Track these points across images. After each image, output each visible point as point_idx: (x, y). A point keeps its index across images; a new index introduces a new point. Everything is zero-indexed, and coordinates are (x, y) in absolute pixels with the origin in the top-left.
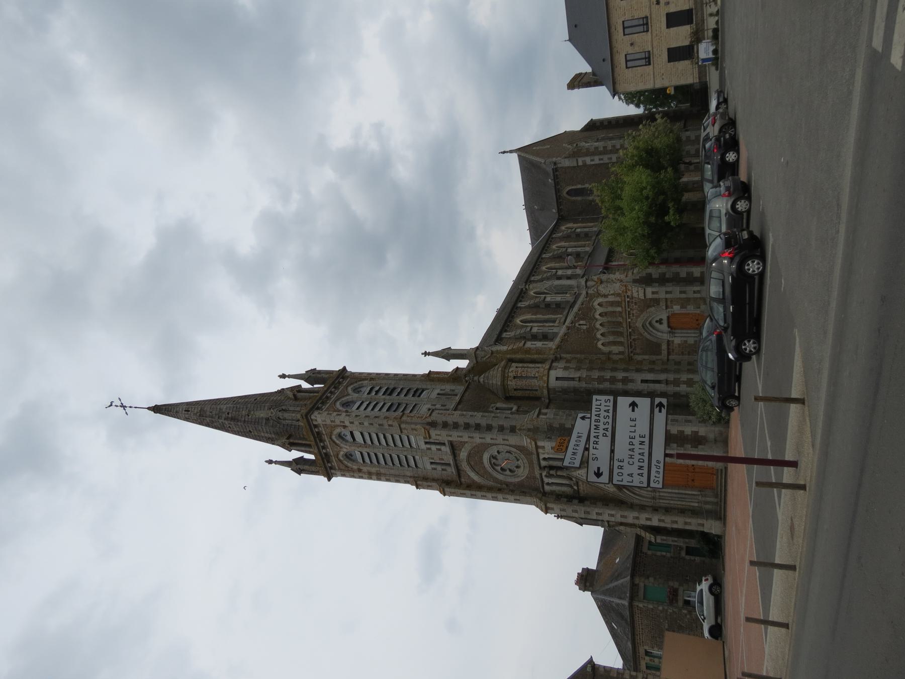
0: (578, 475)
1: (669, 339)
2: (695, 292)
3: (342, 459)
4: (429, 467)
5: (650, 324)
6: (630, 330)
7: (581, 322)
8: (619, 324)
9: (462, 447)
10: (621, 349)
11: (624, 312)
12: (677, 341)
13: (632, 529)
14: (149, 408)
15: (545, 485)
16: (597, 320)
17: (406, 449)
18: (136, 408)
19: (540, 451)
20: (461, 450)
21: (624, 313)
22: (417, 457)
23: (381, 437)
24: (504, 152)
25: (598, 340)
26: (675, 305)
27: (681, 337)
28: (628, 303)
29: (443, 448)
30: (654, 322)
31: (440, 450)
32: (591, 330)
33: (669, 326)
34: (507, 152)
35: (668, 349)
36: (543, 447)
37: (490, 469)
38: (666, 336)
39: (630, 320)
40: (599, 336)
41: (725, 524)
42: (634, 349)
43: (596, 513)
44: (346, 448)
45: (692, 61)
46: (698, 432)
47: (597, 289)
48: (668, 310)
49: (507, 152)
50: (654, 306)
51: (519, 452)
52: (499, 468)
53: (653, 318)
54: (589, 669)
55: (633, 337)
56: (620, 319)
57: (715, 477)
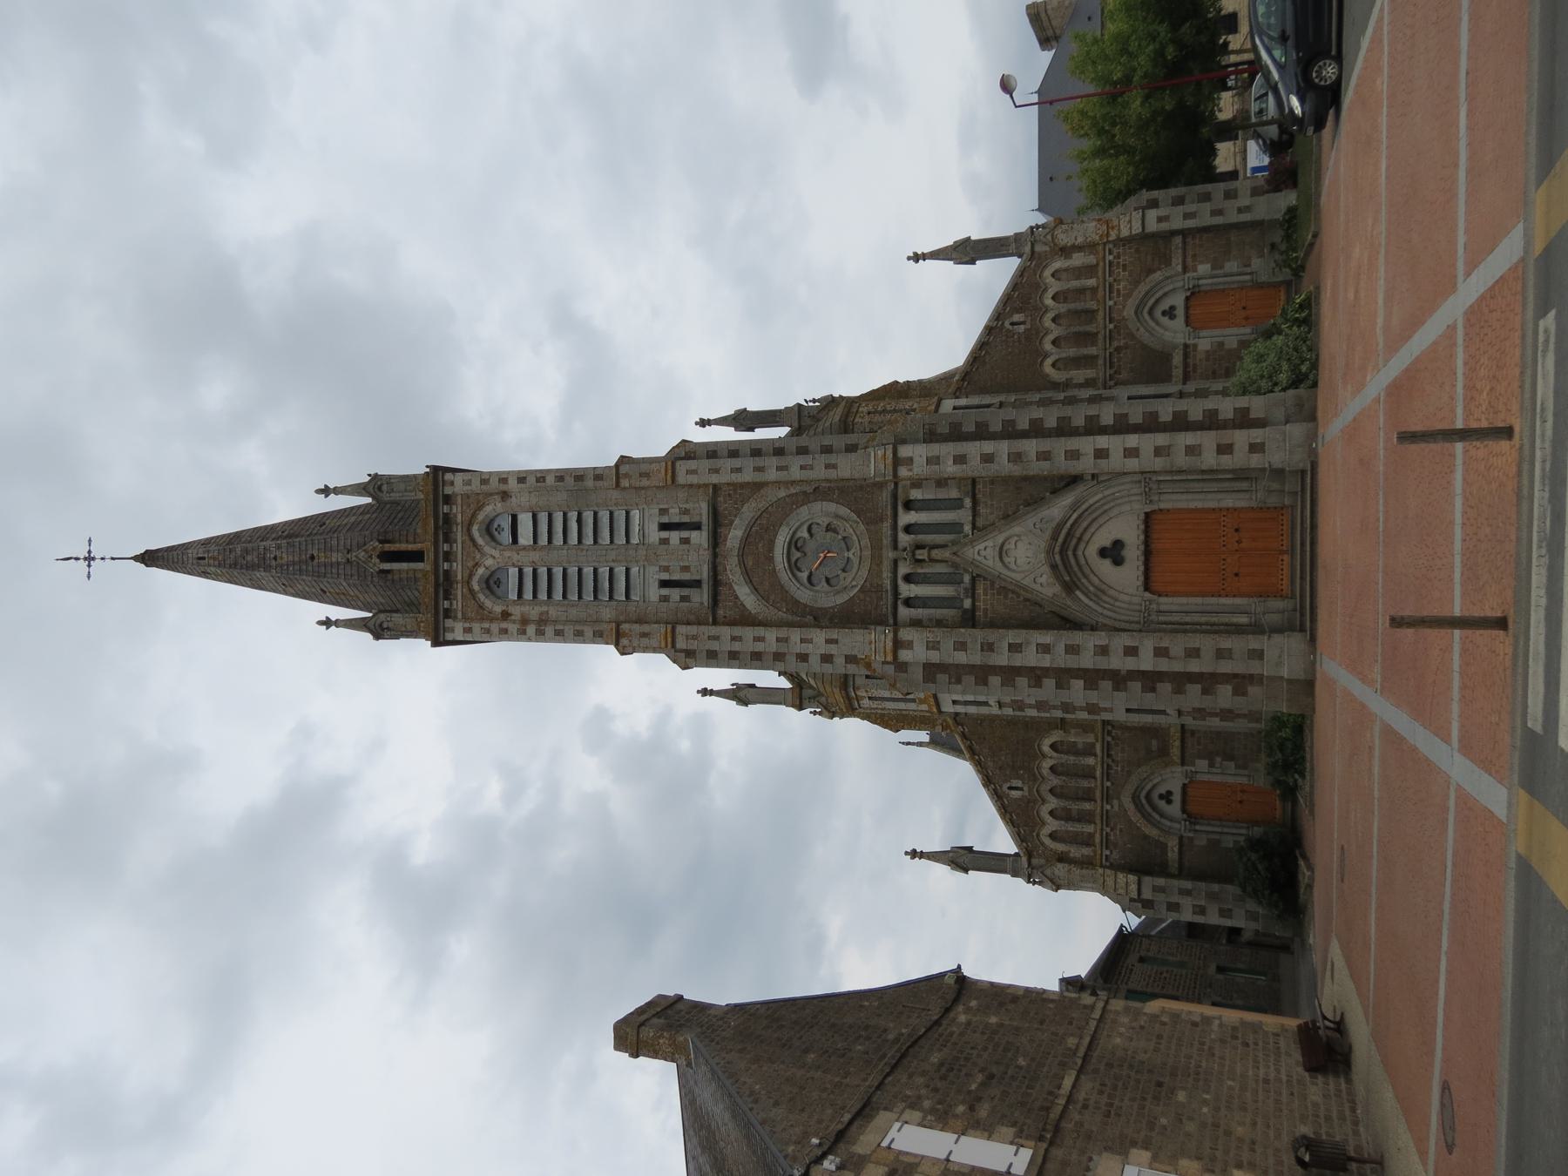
0: (976, 557)
1: (1188, 342)
2: (1240, 210)
3: (476, 587)
4: (654, 593)
5: (1148, 797)
6: (1111, 326)
7: (1017, 317)
8: (1090, 314)
9: (736, 516)
10: (1090, 373)
11: (1099, 766)
12: (1204, 344)
13: (1084, 871)
14: (136, 558)
15: (899, 602)
16: (1044, 756)
17: (616, 547)
18: (113, 559)
19: (903, 472)
20: (731, 523)
21: (1101, 289)
22: (634, 570)
23: (573, 516)
24: (908, 744)
25: (1046, 356)
26: (1201, 262)
27: (1208, 832)
28: (1110, 266)
29: (694, 536)
30: (1155, 796)
31: (686, 541)
32: (1035, 334)
33: (1184, 811)
34: (913, 744)
35: (1186, 365)
36: (910, 461)
37: (784, 576)
38: (1180, 339)
39: (1111, 303)
40: (1048, 346)
41: (1313, 640)
42: (1115, 372)
43: (1010, 645)
44: (492, 558)
45: (1235, 144)
46: (1248, 409)
47: (1052, 235)
48: (1187, 275)
49: (913, 744)
50: (1160, 269)
51: (855, 517)
52: (804, 575)
53: (1154, 787)
54: (950, 980)
55: (1115, 344)
56: (1092, 305)
57: (1286, 557)
